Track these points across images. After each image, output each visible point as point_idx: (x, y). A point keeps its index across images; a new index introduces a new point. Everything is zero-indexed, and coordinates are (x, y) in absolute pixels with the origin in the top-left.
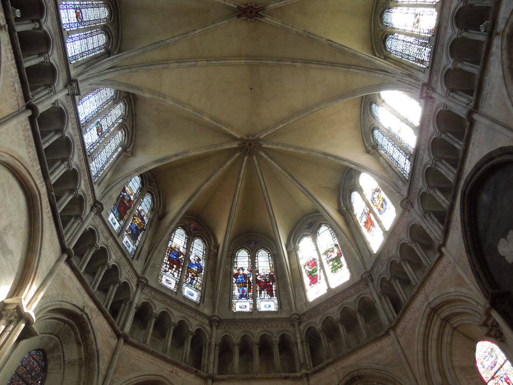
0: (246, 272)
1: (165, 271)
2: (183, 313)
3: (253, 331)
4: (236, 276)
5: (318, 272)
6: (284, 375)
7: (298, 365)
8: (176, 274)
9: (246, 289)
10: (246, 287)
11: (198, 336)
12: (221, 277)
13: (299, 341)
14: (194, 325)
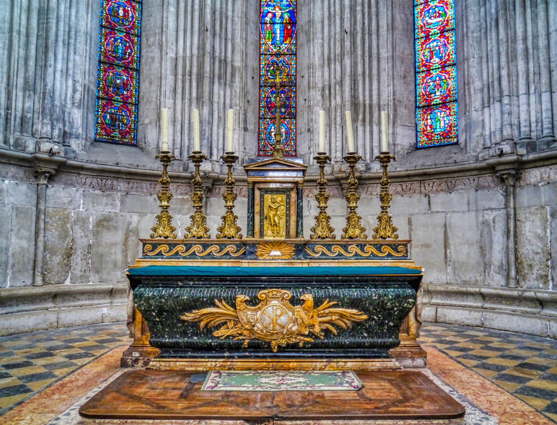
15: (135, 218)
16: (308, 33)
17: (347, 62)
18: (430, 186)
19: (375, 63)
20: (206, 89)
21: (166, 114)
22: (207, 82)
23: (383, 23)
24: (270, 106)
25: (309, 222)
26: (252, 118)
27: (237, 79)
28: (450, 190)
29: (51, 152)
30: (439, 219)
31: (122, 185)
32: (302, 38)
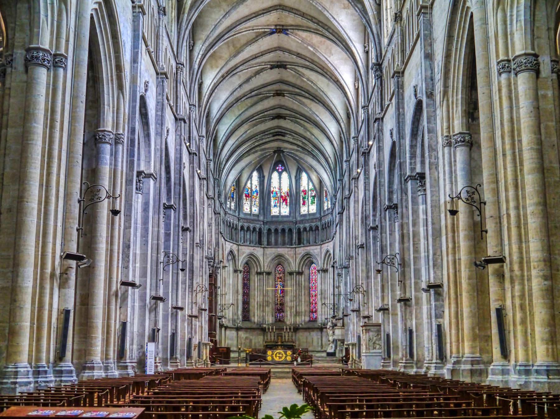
0: (277, 190)
4: (273, 191)
9: (277, 201)
11: (260, 229)
14: (258, 226)
15: (251, 337)
24: (278, 310)
26: (274, 313)
28: (313, 331)
31: (249, 330)
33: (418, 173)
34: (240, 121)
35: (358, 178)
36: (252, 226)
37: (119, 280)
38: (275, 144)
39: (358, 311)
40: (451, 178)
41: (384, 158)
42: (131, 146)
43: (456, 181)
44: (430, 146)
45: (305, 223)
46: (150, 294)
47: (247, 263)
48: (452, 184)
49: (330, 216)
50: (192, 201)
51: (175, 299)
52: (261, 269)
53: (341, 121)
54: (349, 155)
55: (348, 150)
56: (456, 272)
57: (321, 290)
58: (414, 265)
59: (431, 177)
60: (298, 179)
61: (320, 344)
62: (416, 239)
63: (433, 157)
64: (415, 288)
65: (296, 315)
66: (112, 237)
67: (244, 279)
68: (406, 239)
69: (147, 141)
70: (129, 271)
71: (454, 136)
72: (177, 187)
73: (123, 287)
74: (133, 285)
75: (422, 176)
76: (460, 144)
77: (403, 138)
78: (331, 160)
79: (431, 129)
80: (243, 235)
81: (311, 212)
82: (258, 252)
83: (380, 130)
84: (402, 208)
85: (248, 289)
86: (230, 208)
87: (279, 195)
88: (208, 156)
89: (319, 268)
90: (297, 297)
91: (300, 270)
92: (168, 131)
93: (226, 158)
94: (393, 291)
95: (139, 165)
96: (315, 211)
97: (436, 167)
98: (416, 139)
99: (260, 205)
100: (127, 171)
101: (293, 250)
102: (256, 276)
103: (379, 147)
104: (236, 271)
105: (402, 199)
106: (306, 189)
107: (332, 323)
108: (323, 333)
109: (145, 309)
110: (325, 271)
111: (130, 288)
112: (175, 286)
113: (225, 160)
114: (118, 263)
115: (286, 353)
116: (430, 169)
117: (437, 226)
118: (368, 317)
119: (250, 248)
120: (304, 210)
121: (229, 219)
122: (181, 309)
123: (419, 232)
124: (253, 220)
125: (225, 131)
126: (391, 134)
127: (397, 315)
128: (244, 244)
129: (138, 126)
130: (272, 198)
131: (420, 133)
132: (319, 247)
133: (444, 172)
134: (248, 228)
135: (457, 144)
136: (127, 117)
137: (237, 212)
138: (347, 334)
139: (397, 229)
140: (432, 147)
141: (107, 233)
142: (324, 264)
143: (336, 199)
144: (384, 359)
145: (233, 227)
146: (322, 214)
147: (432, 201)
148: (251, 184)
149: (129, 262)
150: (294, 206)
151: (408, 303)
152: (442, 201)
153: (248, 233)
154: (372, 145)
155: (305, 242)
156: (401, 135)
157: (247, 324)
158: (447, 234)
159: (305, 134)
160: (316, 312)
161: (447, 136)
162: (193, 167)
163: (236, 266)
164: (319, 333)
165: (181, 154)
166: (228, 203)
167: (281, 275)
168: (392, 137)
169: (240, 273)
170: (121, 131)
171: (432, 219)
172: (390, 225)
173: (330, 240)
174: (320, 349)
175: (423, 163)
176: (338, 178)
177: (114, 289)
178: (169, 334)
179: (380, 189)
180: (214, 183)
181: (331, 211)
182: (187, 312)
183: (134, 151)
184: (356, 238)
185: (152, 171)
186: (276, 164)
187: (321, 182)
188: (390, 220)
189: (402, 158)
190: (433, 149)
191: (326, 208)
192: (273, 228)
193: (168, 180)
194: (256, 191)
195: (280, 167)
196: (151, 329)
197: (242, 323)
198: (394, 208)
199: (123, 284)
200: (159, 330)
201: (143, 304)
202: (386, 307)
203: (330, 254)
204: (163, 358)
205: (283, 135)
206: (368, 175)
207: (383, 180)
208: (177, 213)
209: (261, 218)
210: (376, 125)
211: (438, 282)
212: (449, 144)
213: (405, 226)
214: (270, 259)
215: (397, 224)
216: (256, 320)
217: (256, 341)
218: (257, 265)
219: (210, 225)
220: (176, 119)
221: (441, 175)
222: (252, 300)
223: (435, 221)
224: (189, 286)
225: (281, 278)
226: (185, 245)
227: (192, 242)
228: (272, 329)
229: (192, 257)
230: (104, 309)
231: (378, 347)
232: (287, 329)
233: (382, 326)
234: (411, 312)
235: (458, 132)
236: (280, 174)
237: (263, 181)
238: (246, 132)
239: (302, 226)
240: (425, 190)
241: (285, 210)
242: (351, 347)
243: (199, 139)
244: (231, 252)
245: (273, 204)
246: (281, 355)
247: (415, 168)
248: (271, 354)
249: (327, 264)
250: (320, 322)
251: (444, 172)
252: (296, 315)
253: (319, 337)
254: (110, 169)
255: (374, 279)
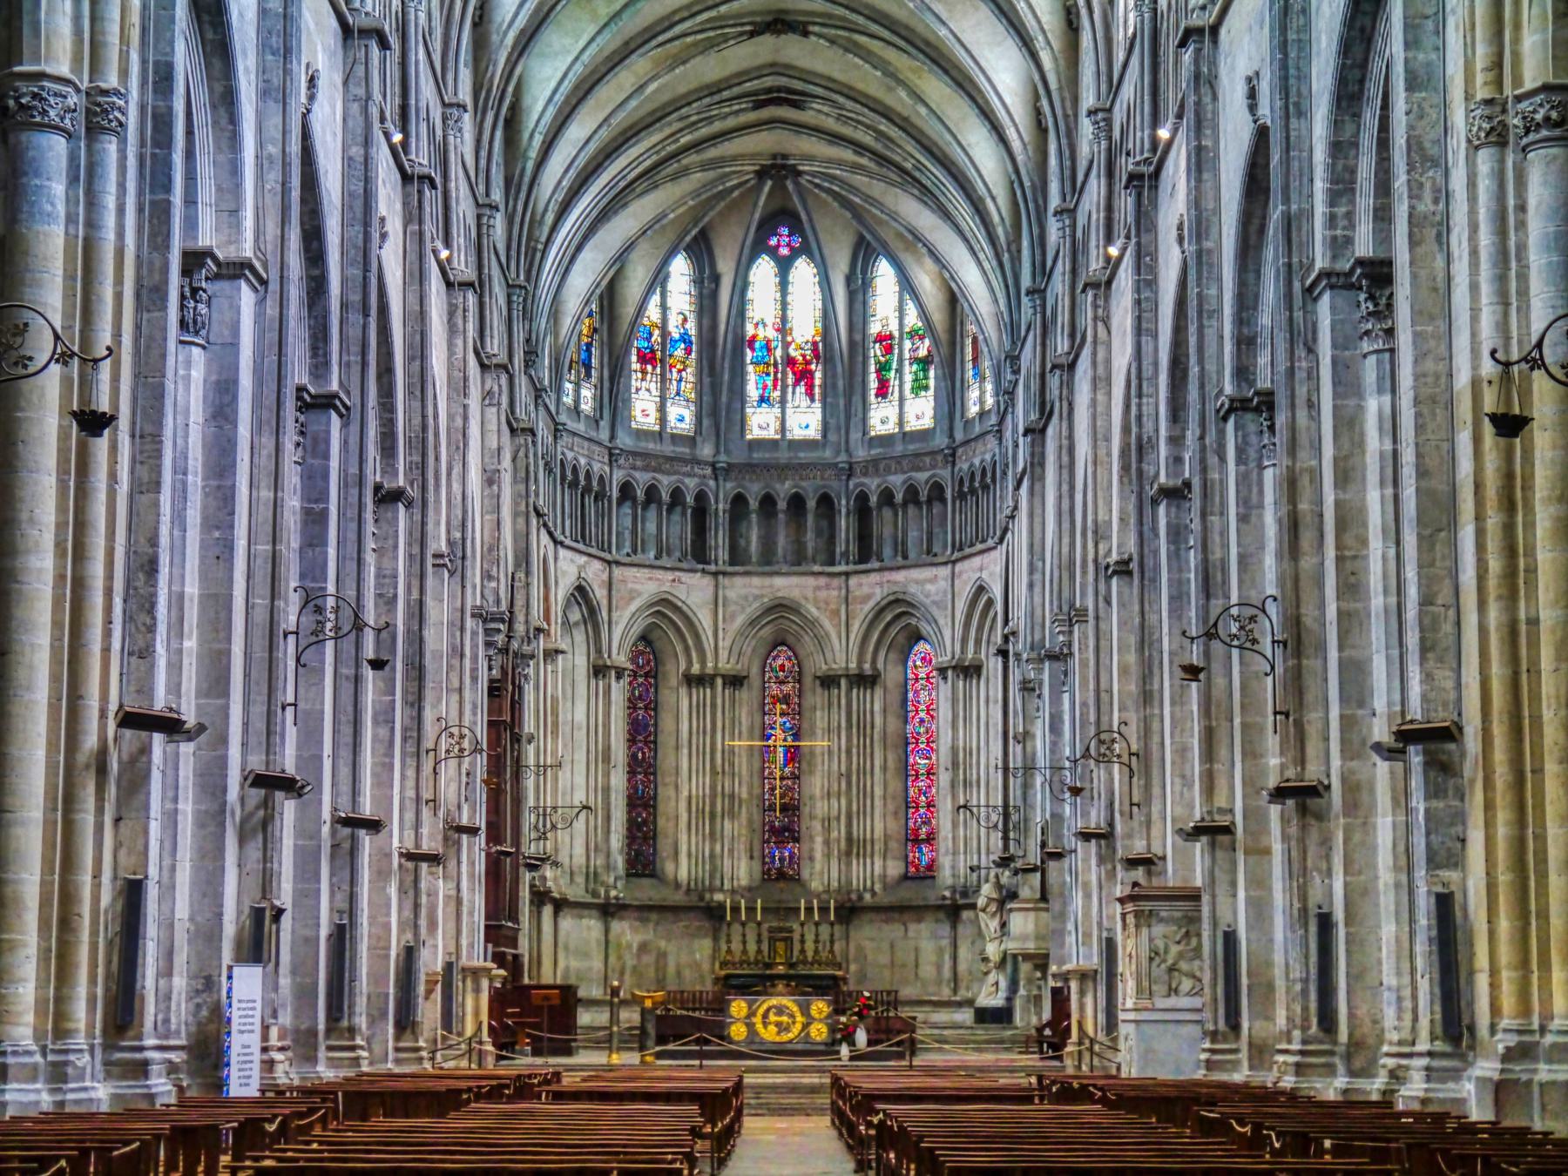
0: (771, 333)
1: (638, 390)
2: (675, 473)
3: (778, 486)
4: (754, 338)
5: (892, 374)
6: (817, 568)
7: (838, 557)
8: (653, 386)
9: (770, 383)
10: (768, 374)
12: (726, 377)
13: (844, 511)
14: (691, 484)
15: (663, 944)
16: (809, 764)
17: (843, 802)
18: (906, 916)
19: (869, 802)
20: (718, 827)
21: (684, 848)
22: (719, 820)
23: (878, 763)
24: (773, 830)
25: (796, 953)
27: (744, 809)
28: (919, 921)
29: (616, 898)
30: (912, 943)
31: (654, 916)
32: (804, 766)
33: (1360, 262)
34: (618, 42)
35: (1109, 283)
36: (666, 482)
37: (113, 707)
38: (763, 143)
39: (1104, 837)
40: (1501, 279)
41: (1218, 199)
42: (156, 144)
43: (1523, 293)
44: (1414, 144)
45: (888, 471)
46: (244, 763)
47: (644, 638)
48: (1506, 304)
49: (992, 442)
50: (416, 380)
51: (345, 788)
52: (703, 662)
53: (1040, 43)
54: (1074, 188)
55: (1068, 163)
56: (1516, 675)
57: (954, 750)
58: (1341, 648)
59: (1414, 276)
60: (859, 288)
61: (947, 972)
62: (1349, 540)
63: (1428, 195)
64: (1344, 741)
65: (848, 853)
66: (81, 526)
67: (632, 705)
68: (1307, 539)
69: (224, 122)
70: (152, 666)
71: (1519, 99)
72: (355, 318)
73: (128, 733)
74: (171, 726)
75: (1378, 274)
76: (1544, 133)
77: (1300, 114)
78: (1000, 207)
79: (1422, 72)
80: (628, 522)
81: (913, 425)
82: (694, 591)
83: (1205, 80)
84: (1293, 406)
85: (653, 743)
86: (576, 410)
87: (779, 353)
88: (482, 188)
89: (944, 659)
90: (852, 780)
91: (867, 666)
92: (312, 82)
93: (560, 196)
94: (1252, 753)
95: (191, 224)
96: (927, 422)
97: (1439, 235)
98: (1357, 116)
99: (700, 395)
100: (139, 247)
101: (836, 582)
102: (683, 691)
103: (1199, 149)
104: (599, 671)
105: (1291, 372)
106: (894, 327)
107: (999, 886)
108: (960, 929)
109: (222, 825)
110: (970, 671)
111: (158, 738)
112: (347, 730)
113: (554, 207)
114: (108, 634)
115: (805, 1010)
116: (1413, 242)
117: (1438, 484)
118: (1146, 862)
119: (659, 574)
120: (882, 418)
121: (570, 455)
122: (374, 826)
123: (1362, 510)
124: (670, 459)
125: (553, 84)
126: (1252, 94)
127: (1267, 852)
128: (634, 559)
129: (183, 55)
130: (750, 368)
131: (1373, 90)
132: (944, 572)
133: (1474, 253)
134: (652, 493)
135: (1532, 137)
136: (135, 18)
137: (605, 424)
138: (1060, 934)
139: (1269, 498)
140: (1421, 148)
141: (61, 509)
142: (964, 641)
143: (1016, 372)
144: (1214, 1036)
145: (587, 489)
146: (959, 436)
147: (1417, 377)
148: (664, 308)
149: (152, 629)
150: (842, 402)
151: (1312, 803)
152: (1462, 379)
153: (652, 513)
154: (1169, 144)
155: (887, 551)
156: (1293, 104)
157: (647, 891)
158: (1479, 518)
159: (889, 100)
160: (930, 839)
161: (1488, 102)
162: (421, 234)
163: (599, 651)
164: (946, 929)
165: (368, 181)
166: (569, 386)
167: (787, 688)
168: (1253, 108)
169: (619, 677)
170: (112, 80)
171: (1419, 455)
172: (1243, 480)
173: (990, 543)
174: (945, 993)
175: (1383, 216)
176: (1026, 281)
177: (91, 741)
178: (324, 932)
179: (1201, 328)
180: (509, 302)
181: (994, 420)
182: (397, 838)
183: (168, 165)
184: (1100, 534)
185: (248, 251)
186: (767, 226)
187: (954, 300)
188: (1240, 460)
189: (1294, 196)
190: (1427, 157)
191: (973, 410)
192: (754, 491)
193: (316, 287)
194: (685, 338)
195: (782, 239)
196: (247, 911)
197: (626, 887)
198: (1257, 410)
199: (130, 720)
200: (279, 912)
201: (216, 807)
202: (1223, 820)
203: (990, 602)
204: (297, 1031)
205: (795, 100)
206: (1153, 269)
207: (1213, 292)
208: (354, 428)
209: (706, 451)
210: (1187, 56)
211: (1441, 719)
212: (1498, 137)
213: (1305, 481)
214: (740, 620)
215: (1269, 475)
216: (683, 874)
217: (684, 959)
218: (687, 649)
219: (491, 479)
220: (346, 30)
221: (1461, 270)
222: (666, 793)
223: (1431, 462)
224: (405, 729)
225: (786, 699)
226: (386, 563)
227: (416, 550)
228: (751, 910)
229: (418, 613)
230: (49, 825)
231: (1187, 984)
232: (809, 910)
233: (1206, 899)
234: (1326, 843)
235: (1538, 84)
236: (784, 266)
237: (714, 295)
238: (642, 87)
239: (873, 484)
240: (1390, 332)
241: (804, 419)
242: (1074, 985)
243: (445, 119)
244: (581, 592)
245: (753, 392)
246: (785, 1019)
247: (1349, 241)
248: (744, 1012)
249: (978, 642)
250: (949, 882)
251: (1474, 253)
252: (848, 853)
253: (945, 942)
254: (70, 239)
255: (1173, 703)
